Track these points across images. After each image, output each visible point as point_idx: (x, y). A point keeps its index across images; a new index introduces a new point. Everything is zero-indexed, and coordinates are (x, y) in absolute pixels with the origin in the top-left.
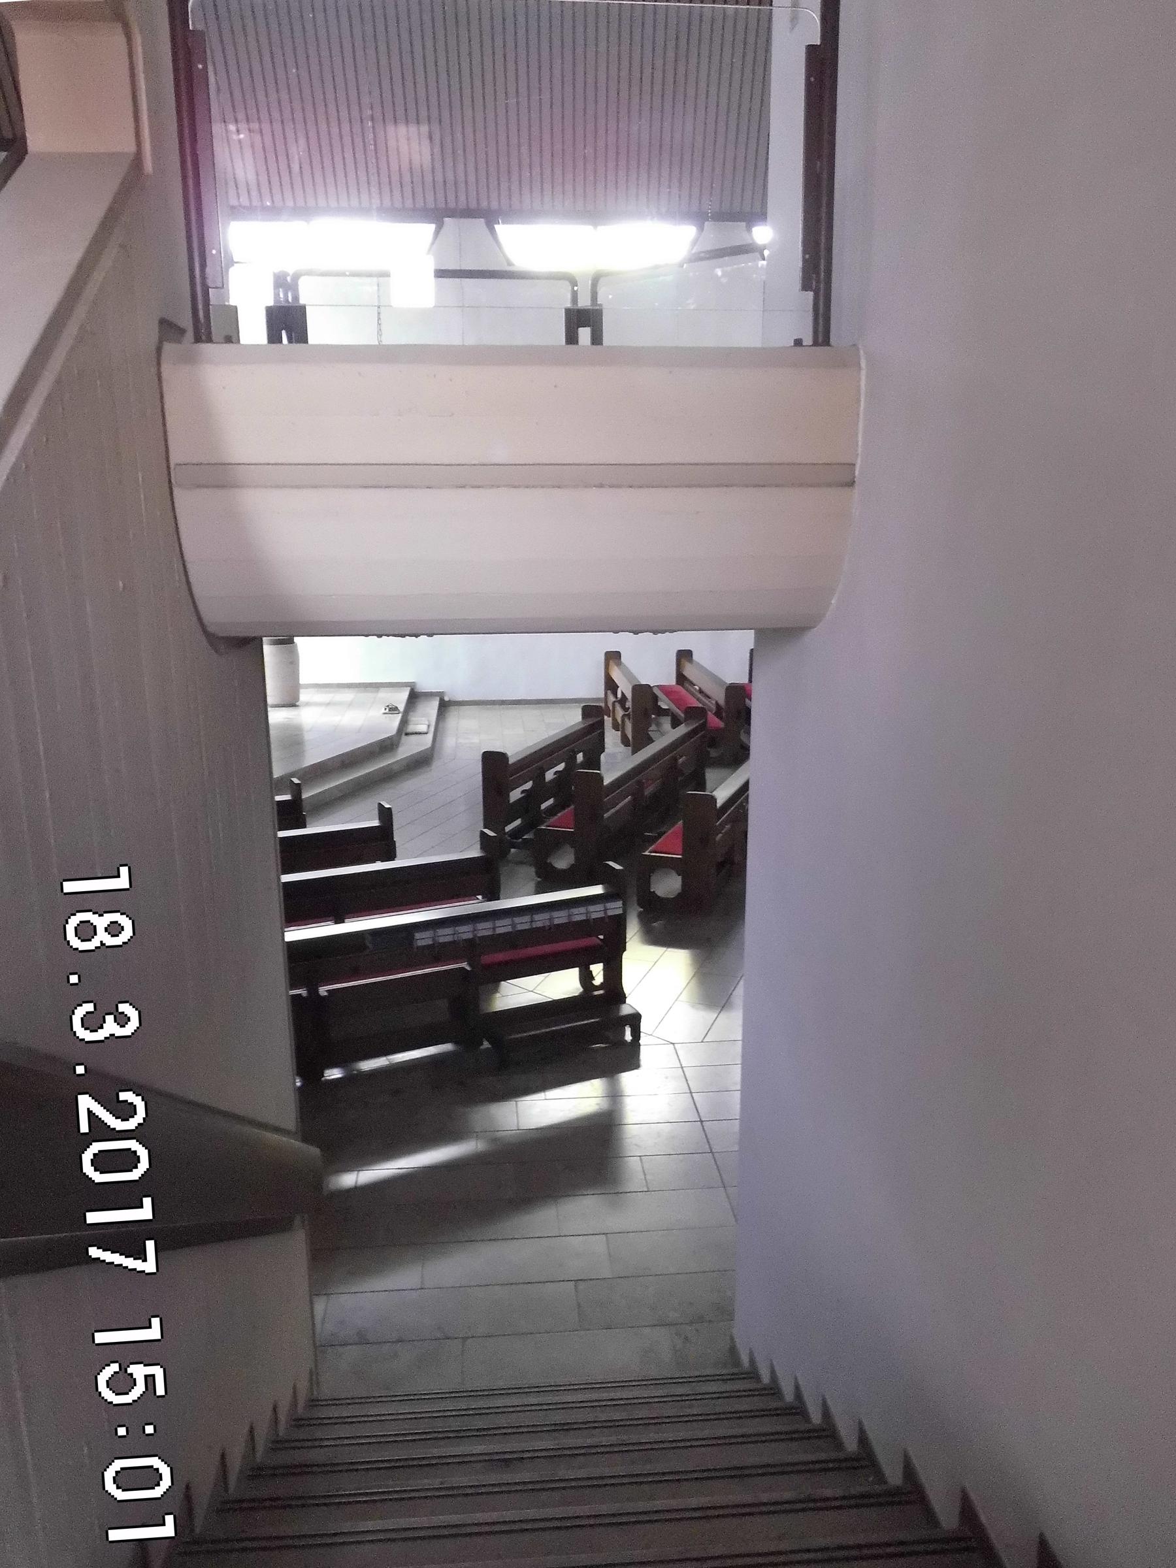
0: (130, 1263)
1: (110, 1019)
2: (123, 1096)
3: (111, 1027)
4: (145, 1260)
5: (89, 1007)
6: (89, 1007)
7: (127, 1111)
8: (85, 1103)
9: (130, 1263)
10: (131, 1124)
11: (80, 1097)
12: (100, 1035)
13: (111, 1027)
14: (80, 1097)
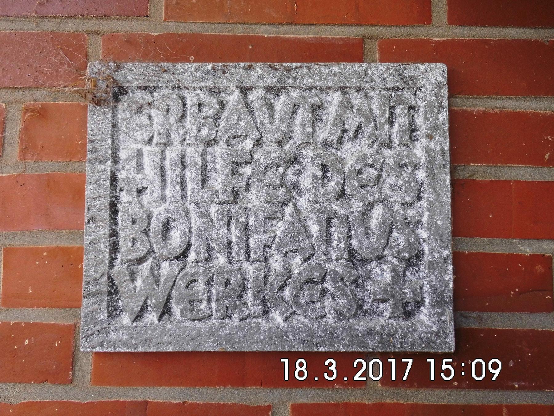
0: (409, 367)
1: (330, 368)
2: (355, 365)
3: (333, 368)
4: (408, 362)
5: (326, 374)
6: (326, 374)
7: (360, 365)
8: (356, 378)
9: (409, 367)
10: (364, 364)
11: (354, 379)
12: (335, 372)
13: (333, 368)
14: (354, 379)
